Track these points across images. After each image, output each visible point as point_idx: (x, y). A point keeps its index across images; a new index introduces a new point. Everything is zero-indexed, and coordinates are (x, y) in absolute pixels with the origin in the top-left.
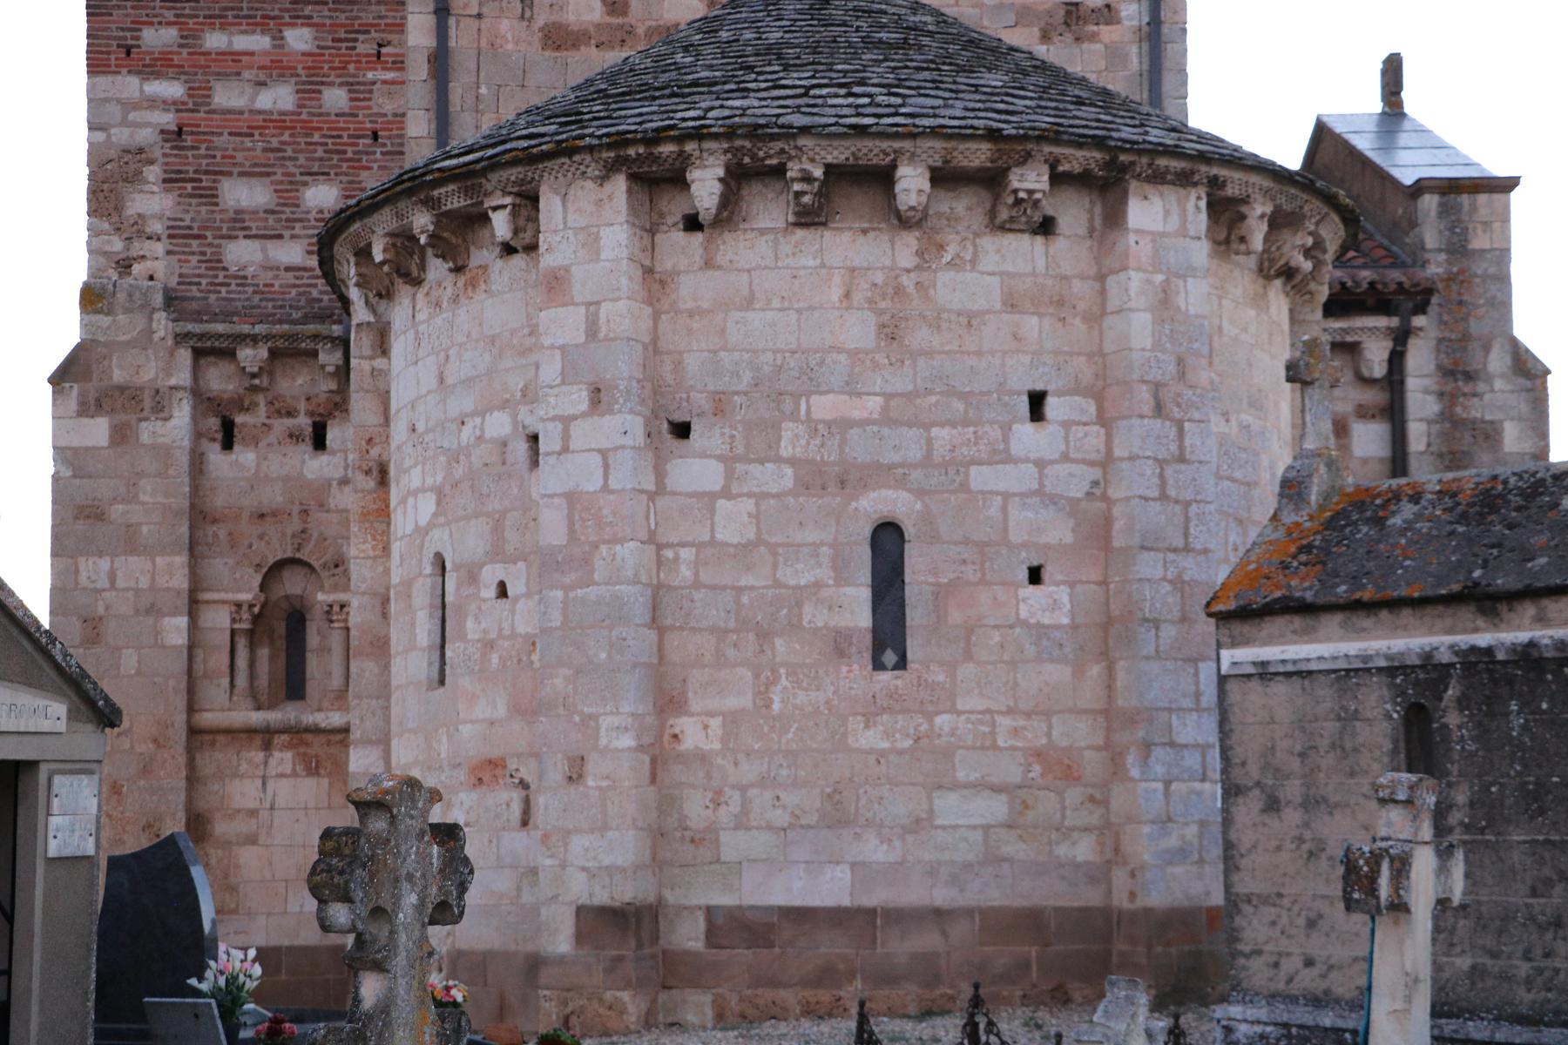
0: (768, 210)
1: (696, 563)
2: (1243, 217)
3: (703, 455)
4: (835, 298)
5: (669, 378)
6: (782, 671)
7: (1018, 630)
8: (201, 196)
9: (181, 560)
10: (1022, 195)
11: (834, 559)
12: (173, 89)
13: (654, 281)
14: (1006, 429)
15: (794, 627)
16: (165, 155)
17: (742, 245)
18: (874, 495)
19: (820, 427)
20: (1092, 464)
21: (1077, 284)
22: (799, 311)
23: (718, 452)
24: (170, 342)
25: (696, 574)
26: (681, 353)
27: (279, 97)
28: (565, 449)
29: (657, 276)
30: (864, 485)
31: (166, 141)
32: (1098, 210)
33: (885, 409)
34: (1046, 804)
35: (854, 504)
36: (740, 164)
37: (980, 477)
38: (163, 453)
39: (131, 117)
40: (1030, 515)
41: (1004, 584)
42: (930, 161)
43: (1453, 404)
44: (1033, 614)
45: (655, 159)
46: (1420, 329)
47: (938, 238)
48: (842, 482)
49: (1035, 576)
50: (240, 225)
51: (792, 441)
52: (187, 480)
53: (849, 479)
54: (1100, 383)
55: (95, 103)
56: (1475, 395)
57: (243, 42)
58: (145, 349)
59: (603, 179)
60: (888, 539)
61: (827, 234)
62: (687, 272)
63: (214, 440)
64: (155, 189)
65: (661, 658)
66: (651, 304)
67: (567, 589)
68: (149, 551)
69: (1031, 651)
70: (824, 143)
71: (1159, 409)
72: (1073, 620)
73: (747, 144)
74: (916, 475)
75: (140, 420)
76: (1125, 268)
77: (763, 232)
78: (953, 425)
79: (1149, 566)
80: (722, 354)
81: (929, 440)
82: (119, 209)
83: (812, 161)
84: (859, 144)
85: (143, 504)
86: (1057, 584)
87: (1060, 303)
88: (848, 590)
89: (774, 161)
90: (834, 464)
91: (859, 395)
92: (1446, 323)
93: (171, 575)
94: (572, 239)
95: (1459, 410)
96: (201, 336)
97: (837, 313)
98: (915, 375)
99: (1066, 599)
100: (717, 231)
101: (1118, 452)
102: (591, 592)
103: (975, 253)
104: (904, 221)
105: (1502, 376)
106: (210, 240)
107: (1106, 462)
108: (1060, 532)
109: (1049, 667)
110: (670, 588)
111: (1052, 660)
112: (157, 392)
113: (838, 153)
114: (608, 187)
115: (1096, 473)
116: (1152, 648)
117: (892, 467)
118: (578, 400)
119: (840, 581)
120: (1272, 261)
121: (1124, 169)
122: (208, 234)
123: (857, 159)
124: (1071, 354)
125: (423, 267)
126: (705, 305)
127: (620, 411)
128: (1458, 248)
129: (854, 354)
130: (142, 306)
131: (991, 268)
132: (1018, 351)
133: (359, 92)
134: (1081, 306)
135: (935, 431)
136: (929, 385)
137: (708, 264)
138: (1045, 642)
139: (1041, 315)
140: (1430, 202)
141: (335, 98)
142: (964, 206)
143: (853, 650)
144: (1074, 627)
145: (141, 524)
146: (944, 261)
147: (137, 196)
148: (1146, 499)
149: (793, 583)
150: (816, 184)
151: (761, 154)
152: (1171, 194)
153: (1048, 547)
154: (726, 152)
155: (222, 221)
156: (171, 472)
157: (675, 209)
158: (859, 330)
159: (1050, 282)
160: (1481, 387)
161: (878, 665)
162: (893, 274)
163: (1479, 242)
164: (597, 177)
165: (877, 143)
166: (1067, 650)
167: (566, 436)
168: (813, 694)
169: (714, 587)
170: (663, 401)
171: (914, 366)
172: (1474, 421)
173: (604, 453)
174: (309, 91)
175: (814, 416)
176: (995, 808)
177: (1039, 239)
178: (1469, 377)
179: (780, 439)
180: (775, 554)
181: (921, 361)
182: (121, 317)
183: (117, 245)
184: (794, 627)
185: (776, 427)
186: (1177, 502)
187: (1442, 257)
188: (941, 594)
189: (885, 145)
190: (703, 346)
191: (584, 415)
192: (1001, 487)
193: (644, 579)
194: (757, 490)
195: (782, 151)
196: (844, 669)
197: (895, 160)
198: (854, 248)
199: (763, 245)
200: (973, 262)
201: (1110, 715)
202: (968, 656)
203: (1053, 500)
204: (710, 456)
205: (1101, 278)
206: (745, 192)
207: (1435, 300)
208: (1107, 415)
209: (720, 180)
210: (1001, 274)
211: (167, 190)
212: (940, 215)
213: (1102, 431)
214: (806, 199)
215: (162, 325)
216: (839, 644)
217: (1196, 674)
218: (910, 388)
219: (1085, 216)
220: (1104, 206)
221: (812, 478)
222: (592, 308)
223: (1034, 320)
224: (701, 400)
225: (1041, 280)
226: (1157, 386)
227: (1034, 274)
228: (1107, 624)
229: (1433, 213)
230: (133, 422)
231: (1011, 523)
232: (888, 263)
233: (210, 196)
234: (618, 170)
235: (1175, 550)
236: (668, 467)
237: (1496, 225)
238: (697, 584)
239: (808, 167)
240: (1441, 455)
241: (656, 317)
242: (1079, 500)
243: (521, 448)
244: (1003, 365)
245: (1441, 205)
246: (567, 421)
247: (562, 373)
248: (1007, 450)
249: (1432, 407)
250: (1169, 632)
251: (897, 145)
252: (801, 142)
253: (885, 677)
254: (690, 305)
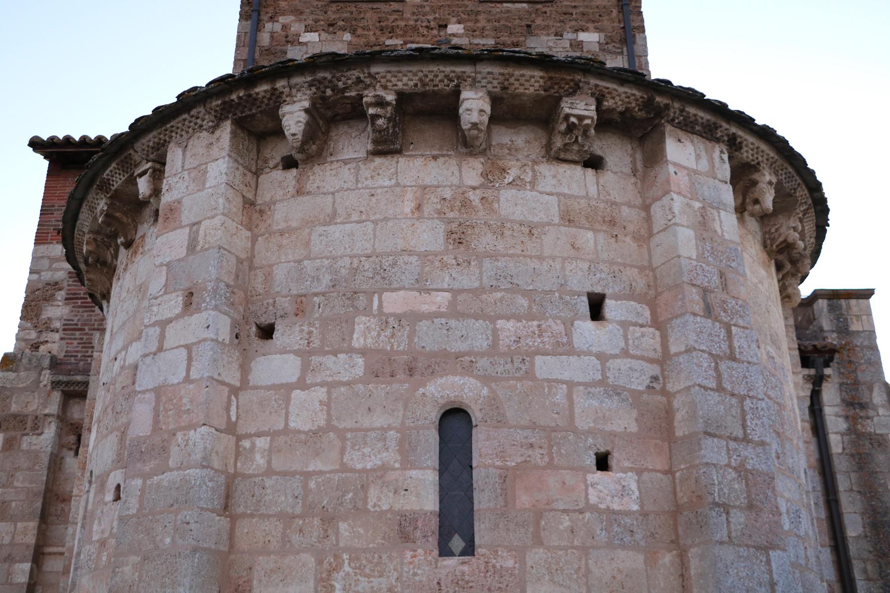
0: (352, 144)
1: (270, 451)
2: (755, 183)
3: (284, 351)
4: (407, 210)
5: (260, 288)
6: (345, 556)
7: (588, 515)
8: (85, 307)
9: (33, 525)
10: (573, 119)
11: (401, 443)
13: (252, 210)
14: (569, 325)
15: (359, 510)
16: (69, 285)
17: (328, 174)
18: (440, 381)
19: (391, 320)
20: (651, 361)
21: (625, 210)
22: (375, 222)
23: (296, 347)
24: (49, 388)
25: (269, 462)
26: (271, 266)
28: (160, 349)
29: (258, 208)
30: (432, 372)
31: (70, 277)
32: (639, 156)
33: (452, 304)
35: (422, 390)
36: (324, 98)
37: (546, 367)
38: (34, 455)
39: (54, 266)
40: (595, 403)
41: (572, 469)
42: (490, 87)
43: (855, 424)
44: (602, 499)
45: (252, 100)
46: (829, 376)
47: (500, 163)
48: (410, 370)
49: (603, 463)
51: (364, 333)
52: (45, 473)
53: (418, 367)
54: (652, 292)
55: (35, 259)
56: (868, 418)
58: (33, 392)
59: (213, 130)
60: (455, 421)
61: (402, 160)
62: (282, 201)
63: (71, 449)
64: (60, 303)
65: (232, 546)
66: (250, 229)
67: (145, 477)
68: (13, 519)
69: (602, 536)
70: (394, 69)
71: (708, 312)
72: (642, 506)
73: (328, 75)
74: (483, 362)
75: (23, 435)
76: (667, 192)
77: (346, 162)
78: (518, 319)
79: (713, 452)
80: (306, 262)
81: (495, 331)
82: (38, 316)
83: (386, 86)
84: (426, 69)
85: (16, 488)
86: (625, 470)
87: (612, 223)
88: (414, 473)
89: (353, 94)
90: (403, 353)
91: (428, 291)
92: (843, 374)
93: (26, 535)
94: (186, 177)
95: (859, 427)
96: (68, 383)
97: (409, 223)
98: (481, 273)
99: (634, 486)
100: (308, 166)
101: (673, 349)
102: (167, 477)
103: (534, 177)
104: (466, 144)
105: (883, 406)
106: (87, 331)
107: (664, 359)
108: (625, 421)
109: (621, 554)
110: (245, 477)
111: (624, 547)
112: (37, 417)
113: (407, 79)
114: (218, 133)
115: (656, 370)
116: (725, 533)
117: (458, 356)
118: (175, 302)
119: (407, 463)
120: (773, 240)
121: (660, 112)
122: (86, 328)
123: (424, 85)
124: (625, 265)
125: (116, 256)
126: (294, 224)
127: (206, 309)
128: (843, 330)
129: (424, 256)
130: (36, 367)
131: (548, 189)
132: (576, 258)
134: (631, 228)
135: (500, 323)
136: (494, 283)
137: (299, 192)
138: (616, 528)
139: (595, 231)
140: (822, 304)
142: (521, 141)
143: (418, 534)
144: (644, 514)
145: (12, 501)
146: (506, 181)
147: (50, 308)
148: (706, 388)
149: (359, 466)
150: (389, 108)
151: (340, 84)
152: (701, 144)
153: (613, 434)
154: (311, 85)
155: (95, 320)
156: (37, 468)
157: (276, 152)
158: (430, 236)
159: (602, 205)
160: (871, 413)
161: (445, 551)
162: (461, 191)
163: (855, 327)
164: (211, 127)
165: (442, 68)
166: (638, 537)
167: (162, 337)
168: (375, 582)
169: (284, 474)
170: (253, 308)
171: (480, 266)
172: (870, 434)
173: (188, 347)
175: (386, 310)
177: (590, 172)
178: (863, 406)
179: (352, 331)
180: (343, 439)
181: (487, 263)
182: (23, 374)
183: (33, 335)
184: (359, 510)
185: (350, 322)
186: (733, 395)
187: (835, 335)
188: (508, 479)
189: (448, 69)
190: (290, 257)
191: (178, 317)
192: (566, 376)
193: (216, 464)
194: (330, 379)
195: (359, 81)
196: (409, 554)
197: (458, 86)
198: (429, 171)
199: (346, 173)
200: (533, 183)
202: (538, 541)
203: (616, 391)
204: (289, 352)
205: (646, 208)
206: (333, 134)
207: (837, 356)
208: (662, 319)
209: (307, 111)
210: (558, 194)
211: (67, 304)
212: (501, 146)
213: (658, 333)
214: (380, 122)
216: (404, 529)
217: (768, 562)
218: (477, 284)
219: (628, 159)
220: (643, 152)
221: (382, 366)
222: (195, 228)
223: (590, 235)
224: (285, 303)
225: (593, 203)
226: (705, 292)
227: (587, 197)
228: (677, 511)
229: (825, 310)
230: (19, 437)
231: (577, 410)
232: (456, 181)
234: (227, 118)
235: (736, 439)
236: (253, 364)
237: (864, 317)
238: (269, 472)
239: (381, 93)
240: (852, 455)
241: (254, 240)
242: (641, 393)
244: (563, 268)
245: (829, 305)
246: (163, 324)
247: (166, 286)
248: (570, 343)
249: (843, 425)
250: (738, 518)
251: (459, 69)
252: (374, 70)
253: (450, 562)
254: (282, 225)
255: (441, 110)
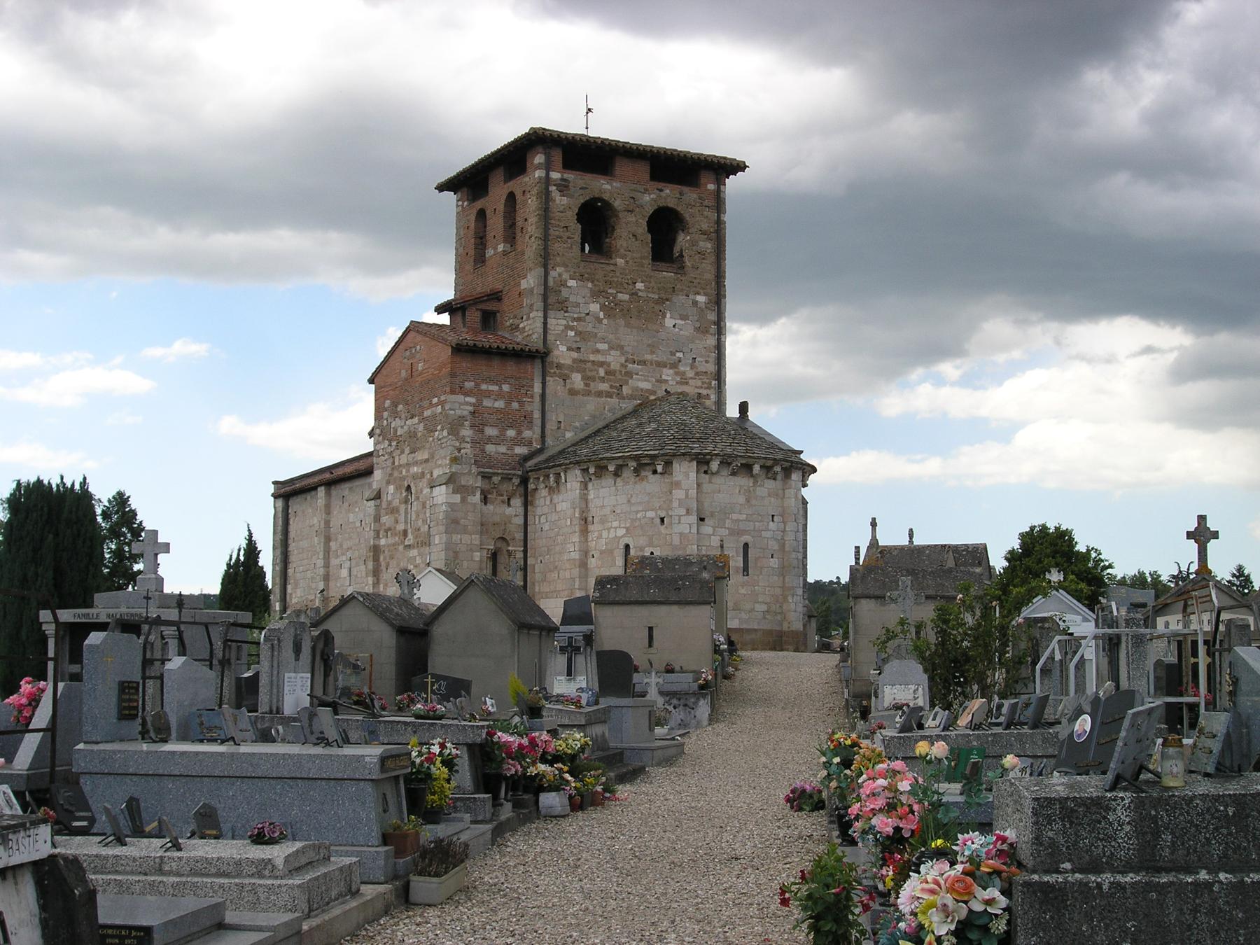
0: (725, 472)
12: (472, 400)
27: (500, 404)
34: (773, 608)
50: (489, 440)
51: (728, 523)
53: (741, 533)
57: (491, 388)
60: (746, 546)
104: (752, 476)
118: (683, 511)
133: (521, 404)
141: (515, 405)
158: (742, 500)
174: (508, 403)
176: (764, 608)
188: (757, 559)
198: (743, 481)
201: (783, 587)
215: (474, 469)
221: (733, 532)
233: (482, 432)
243: (659, 521)
255: (747, 468)
